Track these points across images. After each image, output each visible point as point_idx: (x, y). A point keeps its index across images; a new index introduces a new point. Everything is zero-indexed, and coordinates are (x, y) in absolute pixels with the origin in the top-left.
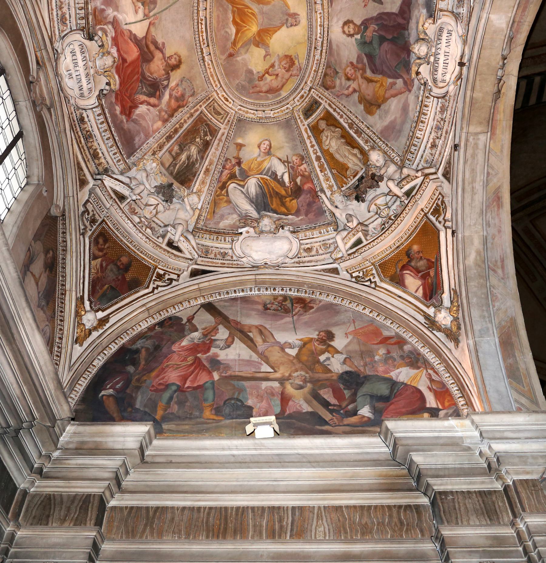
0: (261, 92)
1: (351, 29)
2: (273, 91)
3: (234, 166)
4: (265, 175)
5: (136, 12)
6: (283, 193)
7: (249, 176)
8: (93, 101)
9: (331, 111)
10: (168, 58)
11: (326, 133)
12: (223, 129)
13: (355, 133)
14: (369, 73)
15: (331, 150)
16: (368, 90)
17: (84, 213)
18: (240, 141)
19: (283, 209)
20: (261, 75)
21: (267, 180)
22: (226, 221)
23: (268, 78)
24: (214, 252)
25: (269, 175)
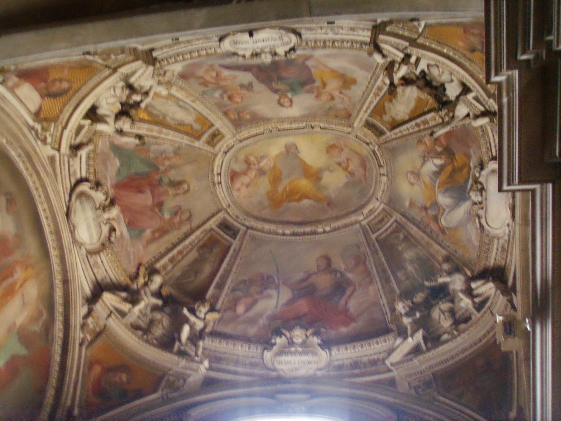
0: (365, 176)
1: (285, 101)
2: (363, 163)
3: (427, 213)
4: (436, 184)
5: (270, 296)
6: (449, 168)
7: (436, 201)
8: (324, 354)
9: (369, 111)
10: (318, 269)
11: (394, 116)
12: (397, 216)
13: (381, 91)
14: (318, 83)
15: (408, 111)
16: (333, 86)
17: (415, 391)
18: (407, 204)
19: (465, 170)
20: (348, 175)
21: (439, 183)
22: (473, 237)
23: (351, 167)
24: (500, 259)
25: (435, 179)
